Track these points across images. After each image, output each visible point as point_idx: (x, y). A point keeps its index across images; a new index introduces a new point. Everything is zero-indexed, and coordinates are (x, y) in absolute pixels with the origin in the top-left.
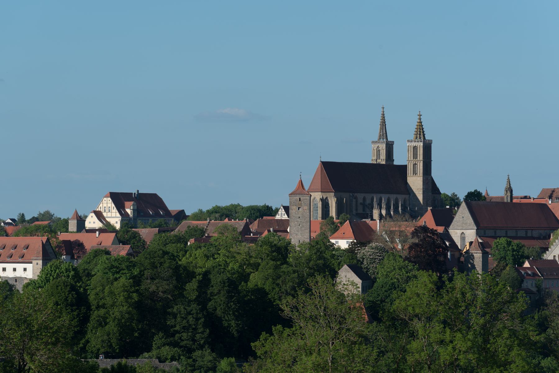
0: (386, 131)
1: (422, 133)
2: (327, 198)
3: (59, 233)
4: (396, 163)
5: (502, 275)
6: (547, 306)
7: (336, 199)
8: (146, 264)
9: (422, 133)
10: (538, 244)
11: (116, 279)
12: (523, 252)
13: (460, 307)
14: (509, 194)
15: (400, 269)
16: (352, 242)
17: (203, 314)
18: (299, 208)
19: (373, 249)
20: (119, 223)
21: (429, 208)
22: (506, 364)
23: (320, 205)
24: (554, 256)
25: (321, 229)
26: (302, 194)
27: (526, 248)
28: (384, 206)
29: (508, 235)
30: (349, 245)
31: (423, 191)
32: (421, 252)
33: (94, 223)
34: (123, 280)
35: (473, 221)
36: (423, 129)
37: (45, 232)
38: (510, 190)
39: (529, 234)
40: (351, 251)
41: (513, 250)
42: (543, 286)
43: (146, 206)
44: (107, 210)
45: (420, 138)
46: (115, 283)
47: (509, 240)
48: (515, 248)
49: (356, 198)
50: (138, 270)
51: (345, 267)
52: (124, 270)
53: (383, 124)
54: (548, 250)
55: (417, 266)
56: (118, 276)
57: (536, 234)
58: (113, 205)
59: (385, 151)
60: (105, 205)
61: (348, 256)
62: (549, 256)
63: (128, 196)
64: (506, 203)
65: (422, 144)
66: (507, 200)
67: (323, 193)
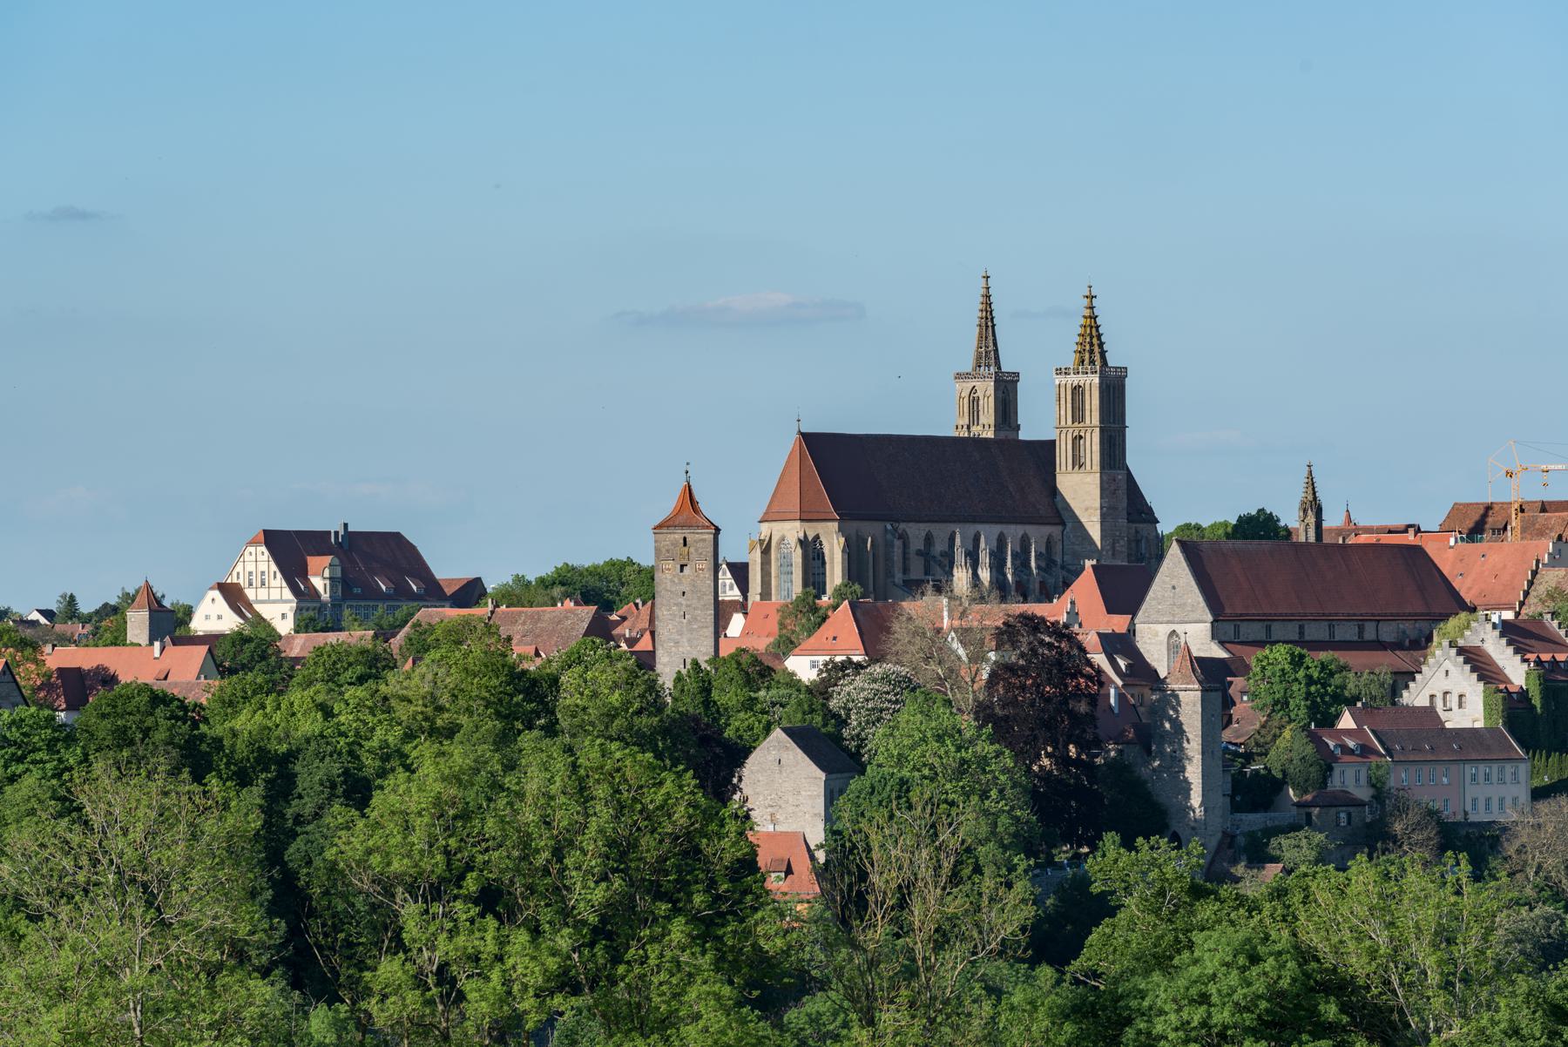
0: (995, 344)
1: (1096, 349)
2: (817, 537)
3: (48, 648)
4: (1023, 435)
5: (1272, 753)
6: (1394, 839)
7: (842, 540)
8: (101, 735)
9: (1096, 349)
10: (1386, 663)
11: (12, 779)
12: (1343, 687)
13: (537, 851)
14: (1311, 519)
15: (939, 738)
16: (826, 664)
17: (270, 878)
18: (682, 567)
19: (875, 681)
20: (291, 616)
21: (1089, 563)
22: (666, 1024)
23: (797, 557)
24: (1432, 697)
25: (782, 625)
26: (690, 527)
27: (1351, 675)
28: (984, 557)
29: (1307, 638)
30: (821, 671)
31: (1103, 516)
32: (1023, 688)
33: (220, 617)
34: (29, 781)
35: (1201, 599)
36: (1099, 336)
37: (7, 647)
38: (1314, 506)
39: (1370, 634)
40: (821, 691)
41: (1310, 680)
42: (1392, 782)
43: (371, 571)
44: (256, 582)
45: (1092, 362)
46: (8, 789)
47: (1298, 650)
48: (1316, 675)
49: (904, 537)
50: (79, 751)
51: (778, 734)
52: (40, 750)
53: (988, 324)
54: (1414, 680)
55: (989, 729)
56: (21, 768)
57: (1388, 632)
58: (274, 567)
59: (992, 400)
60: (250, 567)
61: (800, 704)
62: (1415, 696)
63: (317, 542)
64: (1301, 544)
65: (1096, 380)
66: (1304, 533)
67: (806, 525)
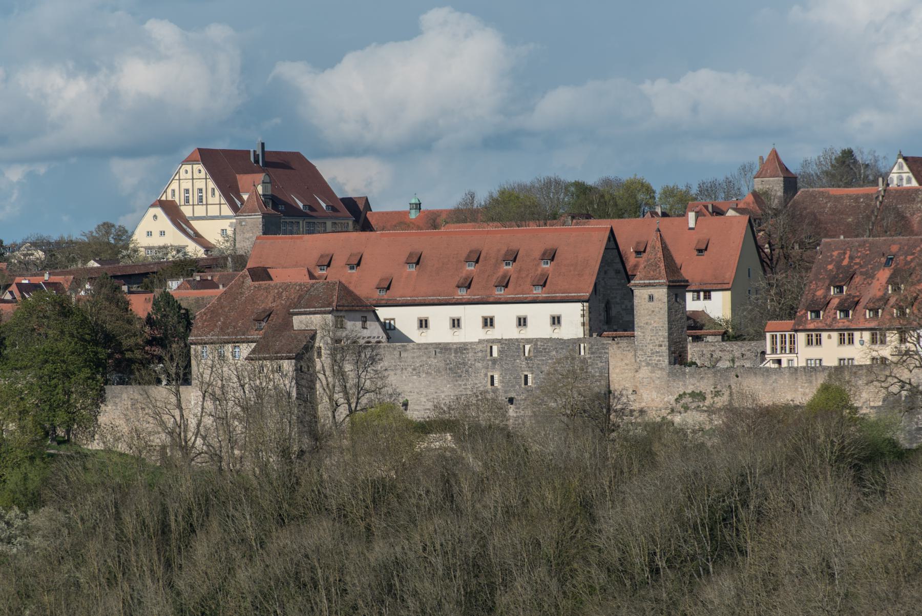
58: (211, 184)
60: (187, 185)
